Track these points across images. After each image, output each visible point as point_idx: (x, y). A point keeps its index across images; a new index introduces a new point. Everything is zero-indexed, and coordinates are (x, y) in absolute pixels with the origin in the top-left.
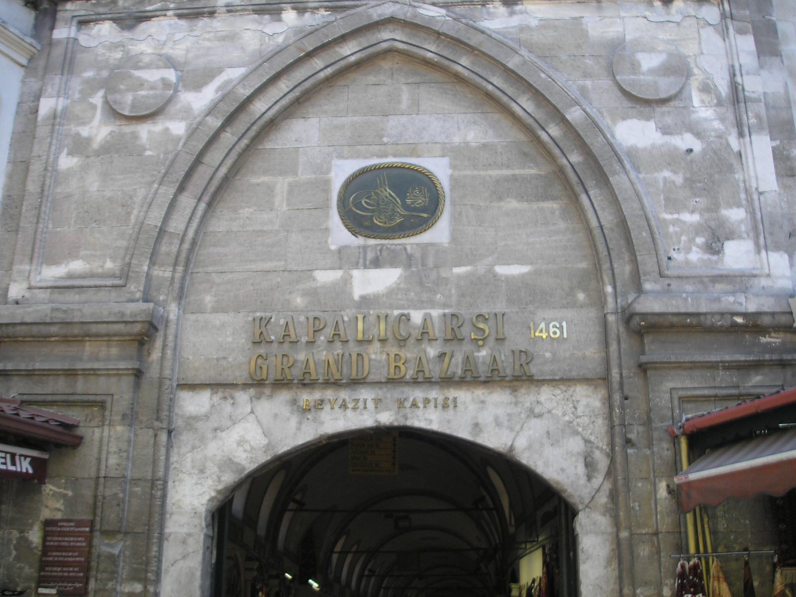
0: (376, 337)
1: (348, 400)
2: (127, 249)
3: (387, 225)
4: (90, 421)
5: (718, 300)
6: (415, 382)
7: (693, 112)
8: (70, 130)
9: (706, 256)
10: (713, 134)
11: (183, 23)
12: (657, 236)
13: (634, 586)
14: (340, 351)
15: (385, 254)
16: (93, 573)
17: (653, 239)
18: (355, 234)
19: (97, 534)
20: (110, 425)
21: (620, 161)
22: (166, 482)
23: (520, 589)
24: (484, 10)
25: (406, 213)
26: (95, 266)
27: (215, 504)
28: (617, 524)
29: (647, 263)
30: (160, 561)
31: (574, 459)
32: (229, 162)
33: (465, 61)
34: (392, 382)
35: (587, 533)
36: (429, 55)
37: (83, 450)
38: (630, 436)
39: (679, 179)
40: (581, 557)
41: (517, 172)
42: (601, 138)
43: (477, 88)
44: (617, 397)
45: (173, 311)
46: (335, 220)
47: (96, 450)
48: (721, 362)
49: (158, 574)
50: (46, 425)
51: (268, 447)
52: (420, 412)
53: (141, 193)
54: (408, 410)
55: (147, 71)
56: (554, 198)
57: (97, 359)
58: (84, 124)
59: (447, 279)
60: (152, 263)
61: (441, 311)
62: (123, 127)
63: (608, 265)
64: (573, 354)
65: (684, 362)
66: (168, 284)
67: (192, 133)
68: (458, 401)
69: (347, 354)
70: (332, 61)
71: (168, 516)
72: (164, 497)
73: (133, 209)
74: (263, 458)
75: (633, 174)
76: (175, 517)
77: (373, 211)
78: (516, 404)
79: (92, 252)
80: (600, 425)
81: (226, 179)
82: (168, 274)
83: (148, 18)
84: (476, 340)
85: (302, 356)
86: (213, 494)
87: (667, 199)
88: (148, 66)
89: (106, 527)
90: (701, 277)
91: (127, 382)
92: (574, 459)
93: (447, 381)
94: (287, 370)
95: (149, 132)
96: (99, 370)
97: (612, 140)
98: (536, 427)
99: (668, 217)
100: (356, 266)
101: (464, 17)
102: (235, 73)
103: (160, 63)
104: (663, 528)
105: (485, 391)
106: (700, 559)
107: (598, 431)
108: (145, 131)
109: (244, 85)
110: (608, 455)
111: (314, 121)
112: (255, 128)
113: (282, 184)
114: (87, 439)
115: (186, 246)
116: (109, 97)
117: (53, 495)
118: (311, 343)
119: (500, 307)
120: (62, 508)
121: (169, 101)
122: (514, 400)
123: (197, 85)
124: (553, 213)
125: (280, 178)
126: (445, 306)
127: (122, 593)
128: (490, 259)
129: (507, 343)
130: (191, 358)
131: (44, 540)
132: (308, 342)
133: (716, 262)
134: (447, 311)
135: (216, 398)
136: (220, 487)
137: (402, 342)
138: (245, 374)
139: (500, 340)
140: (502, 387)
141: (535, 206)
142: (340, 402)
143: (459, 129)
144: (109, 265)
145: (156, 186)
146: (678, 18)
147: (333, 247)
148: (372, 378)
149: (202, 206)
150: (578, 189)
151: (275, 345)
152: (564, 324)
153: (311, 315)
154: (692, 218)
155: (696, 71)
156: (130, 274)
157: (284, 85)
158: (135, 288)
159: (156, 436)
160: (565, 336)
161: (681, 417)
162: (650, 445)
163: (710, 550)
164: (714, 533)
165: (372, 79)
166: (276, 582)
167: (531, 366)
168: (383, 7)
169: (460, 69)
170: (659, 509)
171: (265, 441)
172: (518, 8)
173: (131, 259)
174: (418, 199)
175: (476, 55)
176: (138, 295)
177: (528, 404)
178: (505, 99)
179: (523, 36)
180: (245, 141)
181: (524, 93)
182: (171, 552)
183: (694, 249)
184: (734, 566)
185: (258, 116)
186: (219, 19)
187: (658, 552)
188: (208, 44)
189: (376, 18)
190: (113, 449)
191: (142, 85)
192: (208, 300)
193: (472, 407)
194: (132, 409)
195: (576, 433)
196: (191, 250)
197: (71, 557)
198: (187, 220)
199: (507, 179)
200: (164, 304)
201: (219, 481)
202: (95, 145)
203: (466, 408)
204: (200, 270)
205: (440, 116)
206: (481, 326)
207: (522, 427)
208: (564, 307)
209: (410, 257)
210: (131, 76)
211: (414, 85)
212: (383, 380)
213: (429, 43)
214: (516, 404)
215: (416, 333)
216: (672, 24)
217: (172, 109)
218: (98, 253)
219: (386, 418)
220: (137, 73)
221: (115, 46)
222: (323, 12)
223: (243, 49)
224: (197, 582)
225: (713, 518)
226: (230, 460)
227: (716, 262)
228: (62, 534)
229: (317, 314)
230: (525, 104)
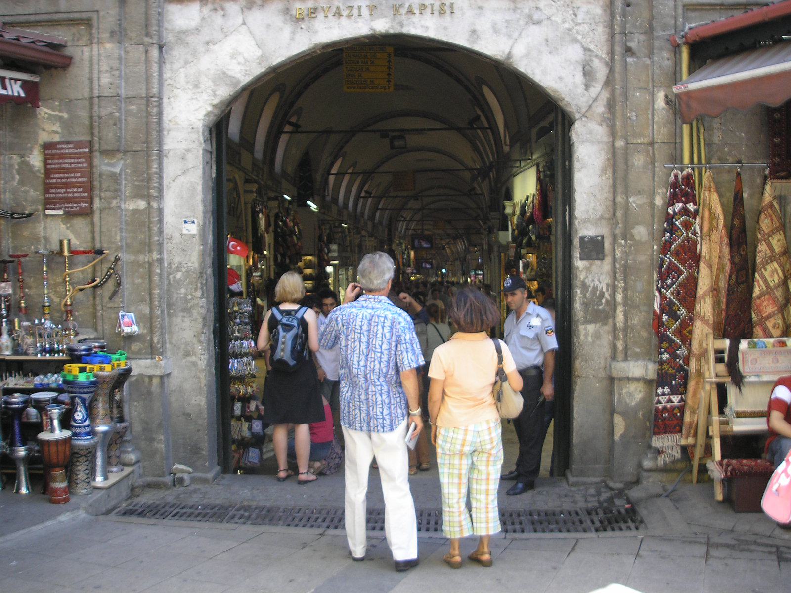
1: (342, 8)
4: (78, 40)
13: (627, 194)
16: (97, 192)
19: (97, 154)
20: (98, 43)
22: (160, 99)
23: (514, 206)
27: (212, 118)
28: (613, 134)
30: (161, 178)
31: (572, 67)
35: (583, 142)
37: (73, 70)
38: (630, 44)
40: (577, 165)
47: (87, 70)
49: (160, 190)
50: (32, 45)
51: (262, 58)
52: (415, 19)
54: (404, 17)
68: (455, 6)
71: (165, 133)
72: (160, 114)
74: (258, 70)
76: (172, 134)
78: (515, 10)
80: (600, 33)
86: (210, 109)
89: (104, 147)
98: (535, 34)
104: (659, 139)
106: (693, 169)
107: (597, 40)
110: (607, 64)
114: (77, 59)
117: (48, 118)
120: (59, 130)
122: (512, 6)
127: (127, 210)
131: (46, 163)
135: (206, 10)
136: (216, 101)
142: (334, 9)
159: (147, 52)
162: (650, 55)
163: (703, 161)
164: (708, 145)
166: (274, 204)
170: (656, 119)
171: (259, 53)
177: (527, 11)
182: (171, 168)
184: (726, 177)
187: (653, 162)
190: (104, 67)
193: (469, 13)
194: (120, 25)
195: (576, 41)
197: (73, 178)
201: (215, 95)
203: (463, 14)
207: (520, 34)
214: (515, 10)
219: (382, 25)
224: (199, 197)
225: (709, 129)
226: (224, 73)
228: (62, 156)
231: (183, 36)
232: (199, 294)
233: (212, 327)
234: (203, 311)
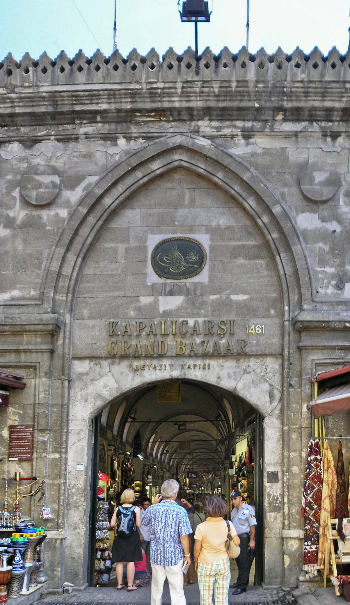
0: (171, 333)
1: (157, 365)
2: (41, 284)
3: (177, 272)
4: (29, 376)
5: (339, 314)
6: (190, 356)
7: (339, 208)
8: (3, 212)
9: (335, 291)
10: (348, 221)
11: (60, 144)
12: (312, 280)
13: (289, 451)
14: (153, 340)
15: (176, 288)
16: (35, 450)
17: (311, 282)
18: (160, 276)
19: (36, 431)
20: (39, 378)
21: (298, 237)
22: (68, 406)
24: (232, 141)
25: (186, 265)
26: (25, 293)
28: (283, 424)
29: (306, 293)
30: (67, 443)
31: (264, 394)
32: (93, 234)
33: (220, 175)
34: (179, 356)
35: (268, 427)
36: (201, 171)
37: (26, 390)
39: (327, 248)
40: (266, 438)
41: (245, 243)
42: (289, 224)
43: (226, 192)
44: (286, 363)
45: (68, 318)
46: (150, 269)
47: (33, 390)
48: (337, 346)
49: (66, 449)
50: (7, 378)
53: (46, 251)
54: (186, 370)
55: (43, 176)
56: (262, 258)
57: (31, 344)
58: (11, 208)
59: (207, 302)
60: (55, 292)
61: (203, 319)
62: (32, 211)
63: (287, 295)
64: (267, 342)
65: (320, 346)
66: (64, 303)
67: (72, 216)
69: (156, 342)
70: (147, 173)
71: (70, 421)
72: (68, 412)
73: (43, 261)
74: (115, 394)
75: (304, 245)
76: (73, 422)
77: (169, 263)
78: (238, 367)
79: (23, 286)
80: (278, 376)
81: (92, 245)
82: (64, 298)
83: (40, 141)
84: (220, 334)
85: (134, 343)
87: (320, 260)
88: (43, 173)
89: (40, 428)
90: (332, 302)
91: (46, 356)
92: (264, 394)
93: (205, 356)
94: (127, 350)
95: (47, 215)
96: (32, 349)
97: (295, 225)
98: (247, 378)
99: (319, 269)
100: (161, 294)
101: (221, 146)
102: (93, 179)
103: (50, 171)
104: (304, 425)
105: (224, 361)
106: (319, 440)
107: (276, 380)
108: (45, 214)
109: (98, 188)
110: (280, 392)
111: (137, 211)
112: (105, 214)
113: (121, 248)
114: (28, 385)
115: (73, 282)
116: (23, 192)
117: (13, 414)
118: (138, 336)
119: (232, 317)
120: (18, 419)
121: (57, 196)
123: (72, 187)
124: (261, 266)
125: (120, 245)
126: (205, 316)
127: (50, 458)
128: (229, 291)
129: (235, 336)
130: (78, 343)
131: (10, 435)
132: (137, 335)
133: (340, 294)
134: (206, 319)
135: (92, 364)
137: (184, 335)
138: (106, 352)
139: (232, 335)
140: (232, 359)
141: (252, 262)
143: (215, 217)
144: (33, 293)
145: (54, 247)
146: (339, 149)
147: (149, 284)
148: (169, 354)
149: (80, 260)
150: (275, 253)
151: (120, 337)
152: (263, 326)
153: (138, 321)
154: (330, 270)
155: (344, 183)
156: (44, 298)
157: (120, 188)
158: (47, 306)
159: (62, 383)
160: (263, 332)
161: (316, 373)
162: (300, 387)
163: (324, 436)
164: (327, 428)
165: (169, 185)
167: (246, 348)
168: (175, 137)
169: (217, 180)
170: (302, 416)
171: (117, 386)
172: (251, 140)
173: (44, 290)
174: (193, 257)
175: (226, 171)
176: (49, 310)
177: (244, 367)
178: (241, 199)
179: (253, 159)
180: (101, 222)
181: (251, 196)
182: (72, 438)
183: (330, 287)
184: (334, 443)
185: (107, 207)
186: (81, 142)
187: (301, 437)
188: (76, 160)
189: (171, 145)
190: (41, 389)
191: (41, 185)
192: (86, 312)
193: (217, 369)
194: (50, 369)
195: (266, 381)
196: (75, 285)
198: (72, 267)
199: (239, 247)
200: (63, 315)
201: (95, 405)
202: (18, 222)
203: (214, 369)
204: (80, 296)
205: (206, 209)
206: (223, 327)
208: (264, 317)
209: (188, 290)
210: (34, 179)
211: (192, 190)
212: (174, 355)
213: (201, 163)
214: (238, 367)
215: (190, 331)
216: (335, 153)
217: (60, 201)
218: (26, 286)
219: (176, 374)
220: (37, 178)
221: (23, 159)
222: (141, 140)
223: (96, 164)
224: (86, 452)
225: (327, 421)
226: (100, 395)
227: (340, 294)
228: (18, 432)
229: (141, 320)
230: (251, 203)
231: (80, 376)
232: (83, 499)
233: (88, 515)
234: (85, 507)
